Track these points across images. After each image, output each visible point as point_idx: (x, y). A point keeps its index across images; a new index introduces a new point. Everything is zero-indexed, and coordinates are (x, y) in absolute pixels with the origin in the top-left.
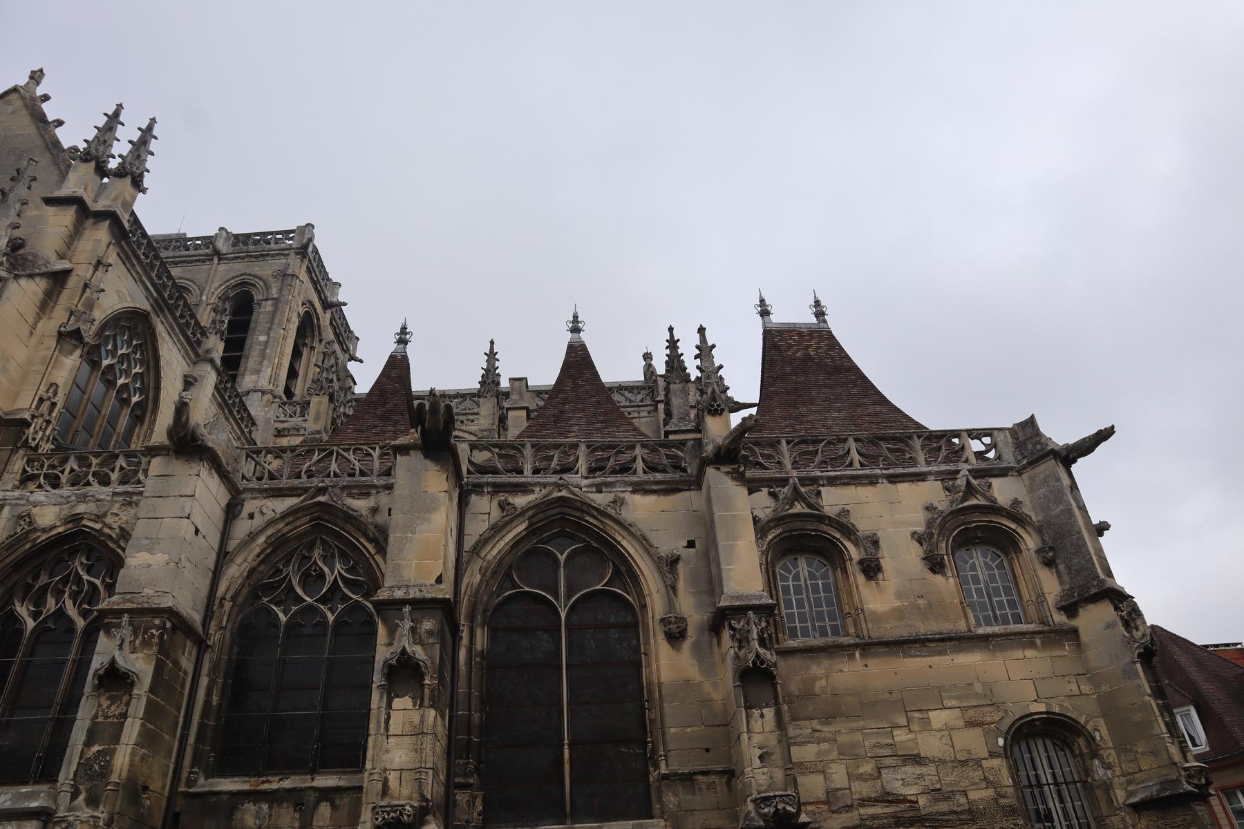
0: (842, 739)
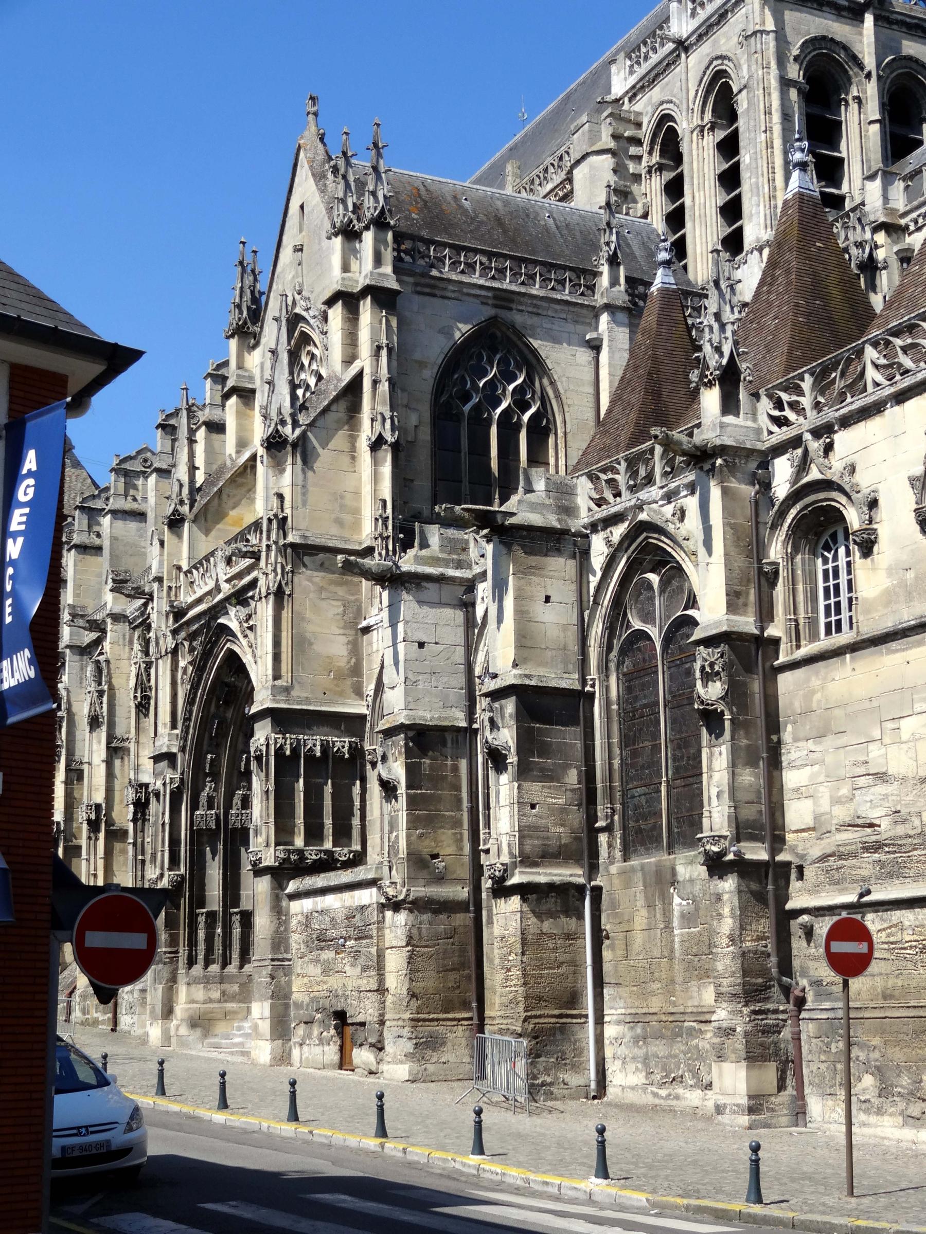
0: (829, 759)
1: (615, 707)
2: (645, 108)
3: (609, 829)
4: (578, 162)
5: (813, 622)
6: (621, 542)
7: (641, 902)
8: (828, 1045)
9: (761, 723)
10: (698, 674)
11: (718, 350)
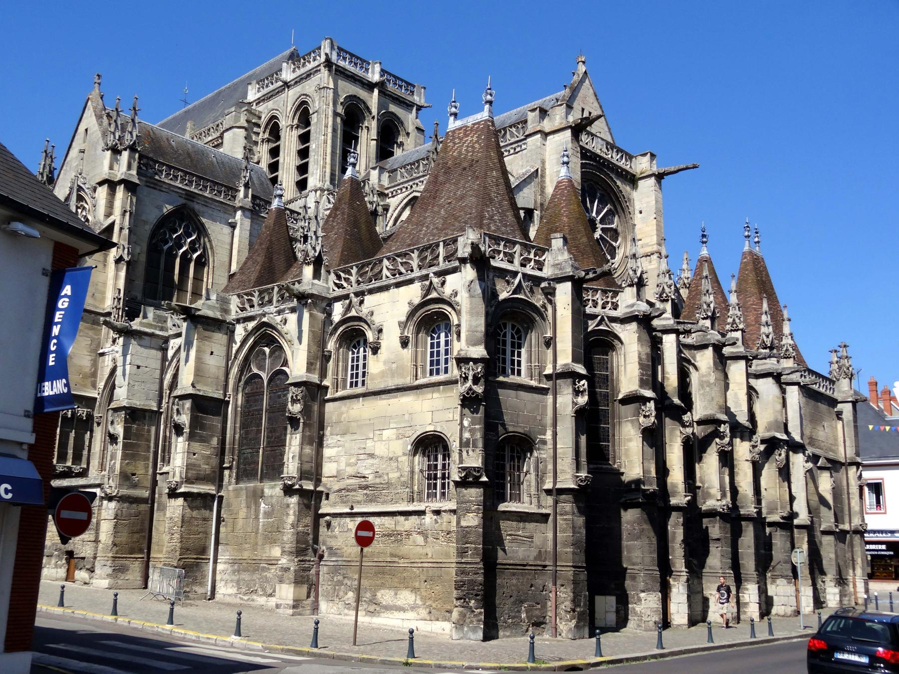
0: (347, 445)
1: (239, 409)
2: (265, 110)
3: (230, 468)
4: (227, 130)
5: (345, 380)
6: (252, 331)
7: (243, 505)
8: (333, 578)
9: (316, 425)
10: (290, 400)
11: (314, 249)
